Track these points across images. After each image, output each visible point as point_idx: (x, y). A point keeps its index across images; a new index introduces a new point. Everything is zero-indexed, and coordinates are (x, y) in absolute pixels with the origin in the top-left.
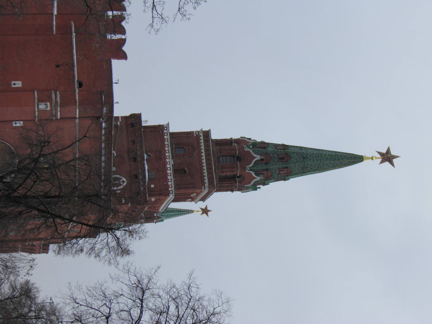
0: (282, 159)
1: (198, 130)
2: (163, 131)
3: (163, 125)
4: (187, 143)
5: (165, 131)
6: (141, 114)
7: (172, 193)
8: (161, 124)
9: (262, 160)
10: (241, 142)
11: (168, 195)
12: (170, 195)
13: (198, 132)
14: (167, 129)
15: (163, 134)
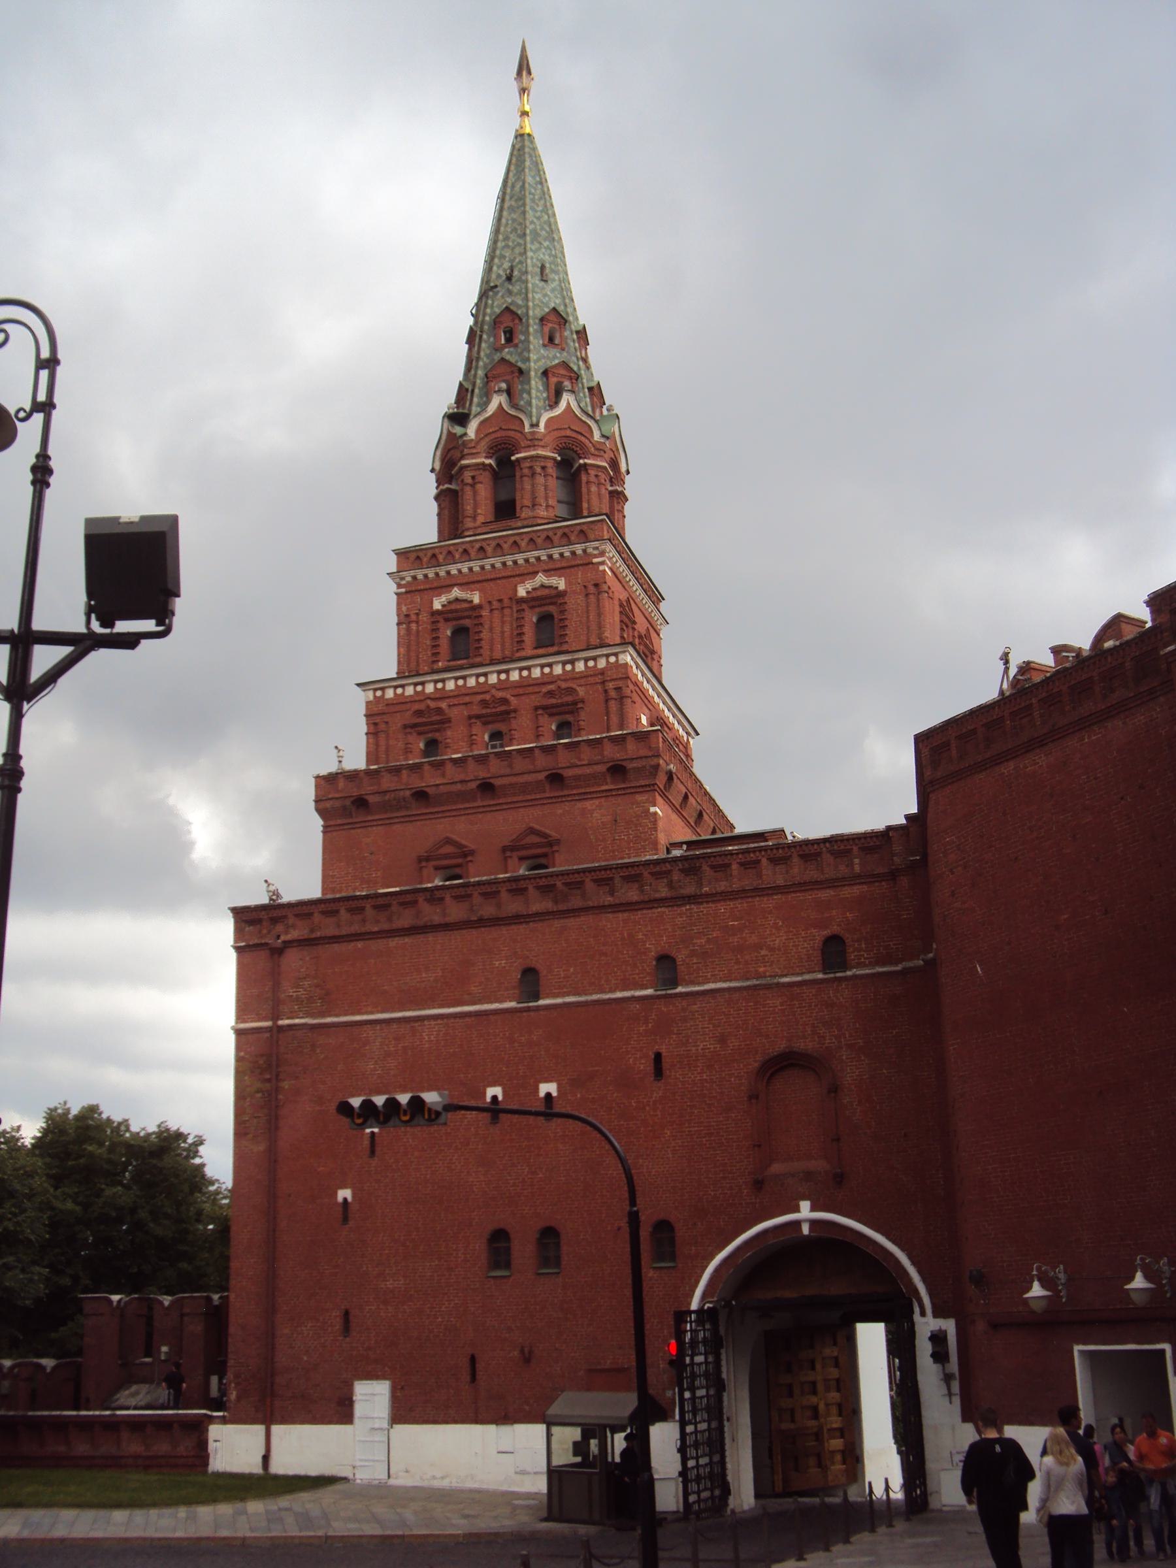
0: (509, 340)
1: (394, 587)
2: (389, 704)
3: (368, 703)
4: (438, 628)
5: (390, 694)
6: (317, 777)
7: (616, 655)
8: (362, 710)
9: (509, 392)
10: (450, 465)
11: (623, 672)
12: (621, 662)
13: (399, 586)
14: (383, 689)
15: (401, 702)
